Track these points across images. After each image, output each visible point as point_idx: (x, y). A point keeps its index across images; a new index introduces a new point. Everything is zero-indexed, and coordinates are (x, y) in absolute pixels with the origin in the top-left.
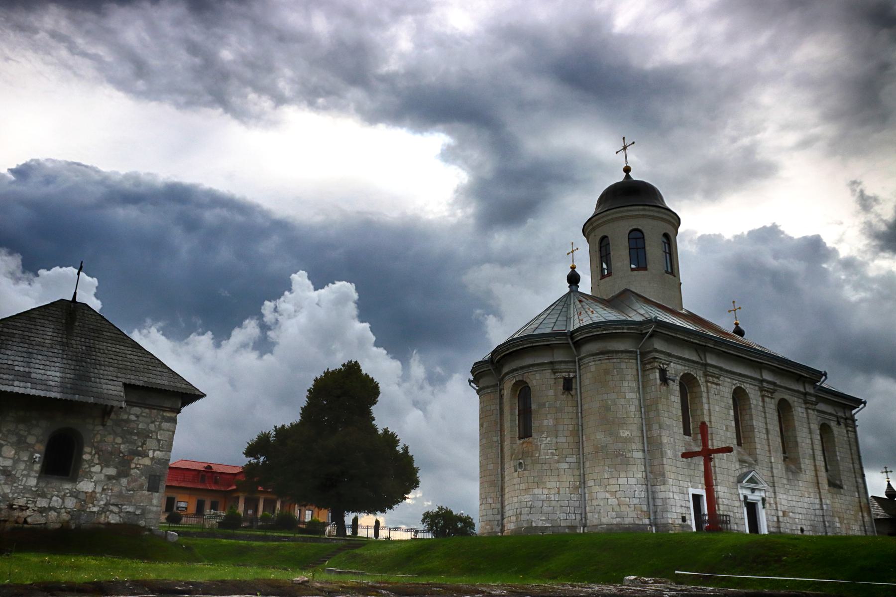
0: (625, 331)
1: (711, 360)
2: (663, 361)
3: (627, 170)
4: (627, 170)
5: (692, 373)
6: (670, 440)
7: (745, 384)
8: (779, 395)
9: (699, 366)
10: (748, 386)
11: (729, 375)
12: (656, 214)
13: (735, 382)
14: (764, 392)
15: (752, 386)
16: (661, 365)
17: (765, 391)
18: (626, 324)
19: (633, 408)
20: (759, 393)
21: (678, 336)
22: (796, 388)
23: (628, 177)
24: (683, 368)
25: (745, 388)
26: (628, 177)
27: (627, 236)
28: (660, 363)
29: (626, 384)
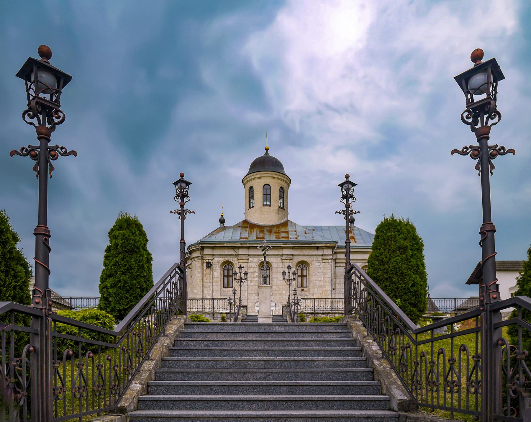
0: (195, 248)
1: (240, 252)
2: (208, 259)
3: (267, 150)
4: (267, 150)
5: (229, 260)
6: (210, 292)
7: (269, 259)
8: (297, 260)
9: (234, 256)
10: (272, 259)
11: (256, 256)
12: (259, 176)
13: (261, 259)
14: (283, 261)
15: (275, 259)
16: (208, 261)
17: (284, 259)
18: (194, 245)
19: (198, 281)
20: (281, 261)
21: (216, 246)
22: (314, 254)
23: (267, 153)
24: (224, 259)
25: (269, 261)
26: (267, 153)
27: (262, 187)
28: (207, 259)
29: (196, 271)
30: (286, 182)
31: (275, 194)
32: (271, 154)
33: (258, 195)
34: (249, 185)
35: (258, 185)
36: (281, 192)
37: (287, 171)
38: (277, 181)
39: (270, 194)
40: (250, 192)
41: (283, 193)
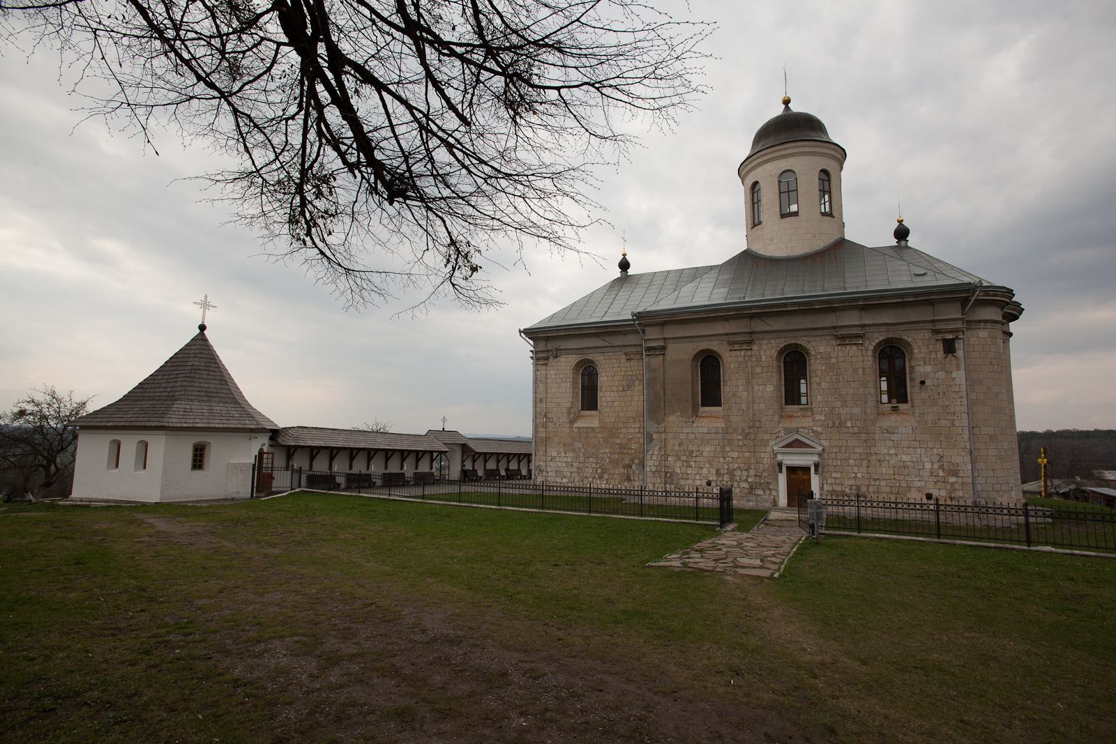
3: (786, 102)
4: (786, 102)
23: (787, 108)
26: (787, 108)
30: (833, 157)
31: (808, 184)
32: (795, 107)
33: (769, 196)
34: (750, 181)
35: (767, 174)
36: (823, 180)
37: (835, 134)
38: (805, 159)
39: (797, 190)
40: (753, 194)
41: (827, 182)
